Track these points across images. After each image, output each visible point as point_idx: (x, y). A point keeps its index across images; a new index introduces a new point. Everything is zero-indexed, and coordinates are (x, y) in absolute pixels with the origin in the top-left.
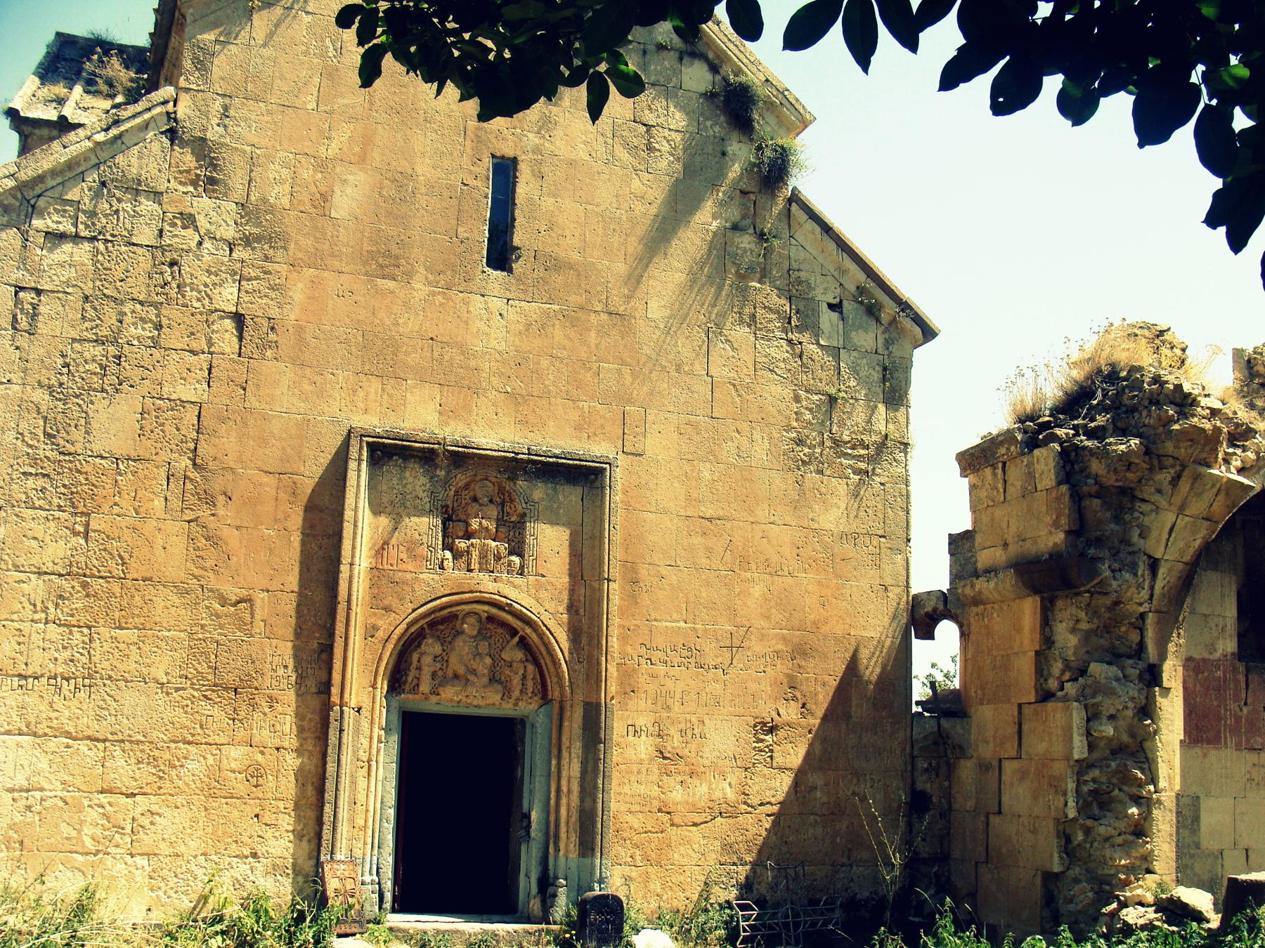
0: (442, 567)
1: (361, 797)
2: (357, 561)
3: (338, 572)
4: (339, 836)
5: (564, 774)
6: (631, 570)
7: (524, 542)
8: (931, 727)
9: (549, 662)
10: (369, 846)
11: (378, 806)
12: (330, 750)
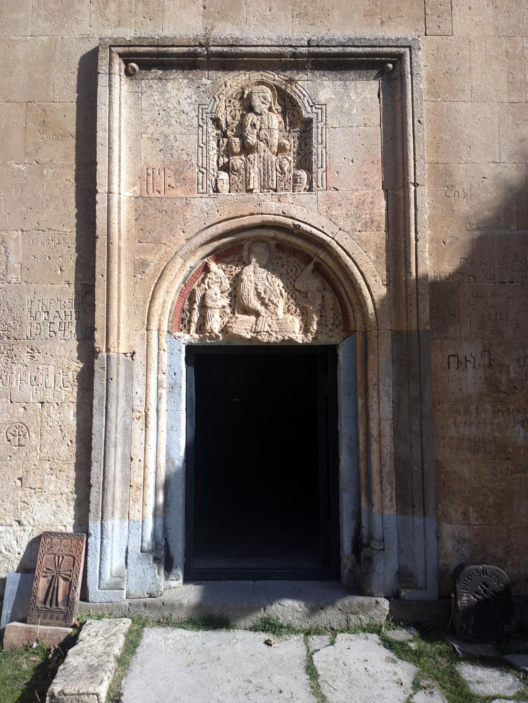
0: (216, 190)
1: (138, 452)
2: (115, 188)
3: (94, 203)
4: (109, 498)
5: (374, 415)
6: (443, 176)
7: (311, 153)
9: (348, 289)
12: (95, 402)
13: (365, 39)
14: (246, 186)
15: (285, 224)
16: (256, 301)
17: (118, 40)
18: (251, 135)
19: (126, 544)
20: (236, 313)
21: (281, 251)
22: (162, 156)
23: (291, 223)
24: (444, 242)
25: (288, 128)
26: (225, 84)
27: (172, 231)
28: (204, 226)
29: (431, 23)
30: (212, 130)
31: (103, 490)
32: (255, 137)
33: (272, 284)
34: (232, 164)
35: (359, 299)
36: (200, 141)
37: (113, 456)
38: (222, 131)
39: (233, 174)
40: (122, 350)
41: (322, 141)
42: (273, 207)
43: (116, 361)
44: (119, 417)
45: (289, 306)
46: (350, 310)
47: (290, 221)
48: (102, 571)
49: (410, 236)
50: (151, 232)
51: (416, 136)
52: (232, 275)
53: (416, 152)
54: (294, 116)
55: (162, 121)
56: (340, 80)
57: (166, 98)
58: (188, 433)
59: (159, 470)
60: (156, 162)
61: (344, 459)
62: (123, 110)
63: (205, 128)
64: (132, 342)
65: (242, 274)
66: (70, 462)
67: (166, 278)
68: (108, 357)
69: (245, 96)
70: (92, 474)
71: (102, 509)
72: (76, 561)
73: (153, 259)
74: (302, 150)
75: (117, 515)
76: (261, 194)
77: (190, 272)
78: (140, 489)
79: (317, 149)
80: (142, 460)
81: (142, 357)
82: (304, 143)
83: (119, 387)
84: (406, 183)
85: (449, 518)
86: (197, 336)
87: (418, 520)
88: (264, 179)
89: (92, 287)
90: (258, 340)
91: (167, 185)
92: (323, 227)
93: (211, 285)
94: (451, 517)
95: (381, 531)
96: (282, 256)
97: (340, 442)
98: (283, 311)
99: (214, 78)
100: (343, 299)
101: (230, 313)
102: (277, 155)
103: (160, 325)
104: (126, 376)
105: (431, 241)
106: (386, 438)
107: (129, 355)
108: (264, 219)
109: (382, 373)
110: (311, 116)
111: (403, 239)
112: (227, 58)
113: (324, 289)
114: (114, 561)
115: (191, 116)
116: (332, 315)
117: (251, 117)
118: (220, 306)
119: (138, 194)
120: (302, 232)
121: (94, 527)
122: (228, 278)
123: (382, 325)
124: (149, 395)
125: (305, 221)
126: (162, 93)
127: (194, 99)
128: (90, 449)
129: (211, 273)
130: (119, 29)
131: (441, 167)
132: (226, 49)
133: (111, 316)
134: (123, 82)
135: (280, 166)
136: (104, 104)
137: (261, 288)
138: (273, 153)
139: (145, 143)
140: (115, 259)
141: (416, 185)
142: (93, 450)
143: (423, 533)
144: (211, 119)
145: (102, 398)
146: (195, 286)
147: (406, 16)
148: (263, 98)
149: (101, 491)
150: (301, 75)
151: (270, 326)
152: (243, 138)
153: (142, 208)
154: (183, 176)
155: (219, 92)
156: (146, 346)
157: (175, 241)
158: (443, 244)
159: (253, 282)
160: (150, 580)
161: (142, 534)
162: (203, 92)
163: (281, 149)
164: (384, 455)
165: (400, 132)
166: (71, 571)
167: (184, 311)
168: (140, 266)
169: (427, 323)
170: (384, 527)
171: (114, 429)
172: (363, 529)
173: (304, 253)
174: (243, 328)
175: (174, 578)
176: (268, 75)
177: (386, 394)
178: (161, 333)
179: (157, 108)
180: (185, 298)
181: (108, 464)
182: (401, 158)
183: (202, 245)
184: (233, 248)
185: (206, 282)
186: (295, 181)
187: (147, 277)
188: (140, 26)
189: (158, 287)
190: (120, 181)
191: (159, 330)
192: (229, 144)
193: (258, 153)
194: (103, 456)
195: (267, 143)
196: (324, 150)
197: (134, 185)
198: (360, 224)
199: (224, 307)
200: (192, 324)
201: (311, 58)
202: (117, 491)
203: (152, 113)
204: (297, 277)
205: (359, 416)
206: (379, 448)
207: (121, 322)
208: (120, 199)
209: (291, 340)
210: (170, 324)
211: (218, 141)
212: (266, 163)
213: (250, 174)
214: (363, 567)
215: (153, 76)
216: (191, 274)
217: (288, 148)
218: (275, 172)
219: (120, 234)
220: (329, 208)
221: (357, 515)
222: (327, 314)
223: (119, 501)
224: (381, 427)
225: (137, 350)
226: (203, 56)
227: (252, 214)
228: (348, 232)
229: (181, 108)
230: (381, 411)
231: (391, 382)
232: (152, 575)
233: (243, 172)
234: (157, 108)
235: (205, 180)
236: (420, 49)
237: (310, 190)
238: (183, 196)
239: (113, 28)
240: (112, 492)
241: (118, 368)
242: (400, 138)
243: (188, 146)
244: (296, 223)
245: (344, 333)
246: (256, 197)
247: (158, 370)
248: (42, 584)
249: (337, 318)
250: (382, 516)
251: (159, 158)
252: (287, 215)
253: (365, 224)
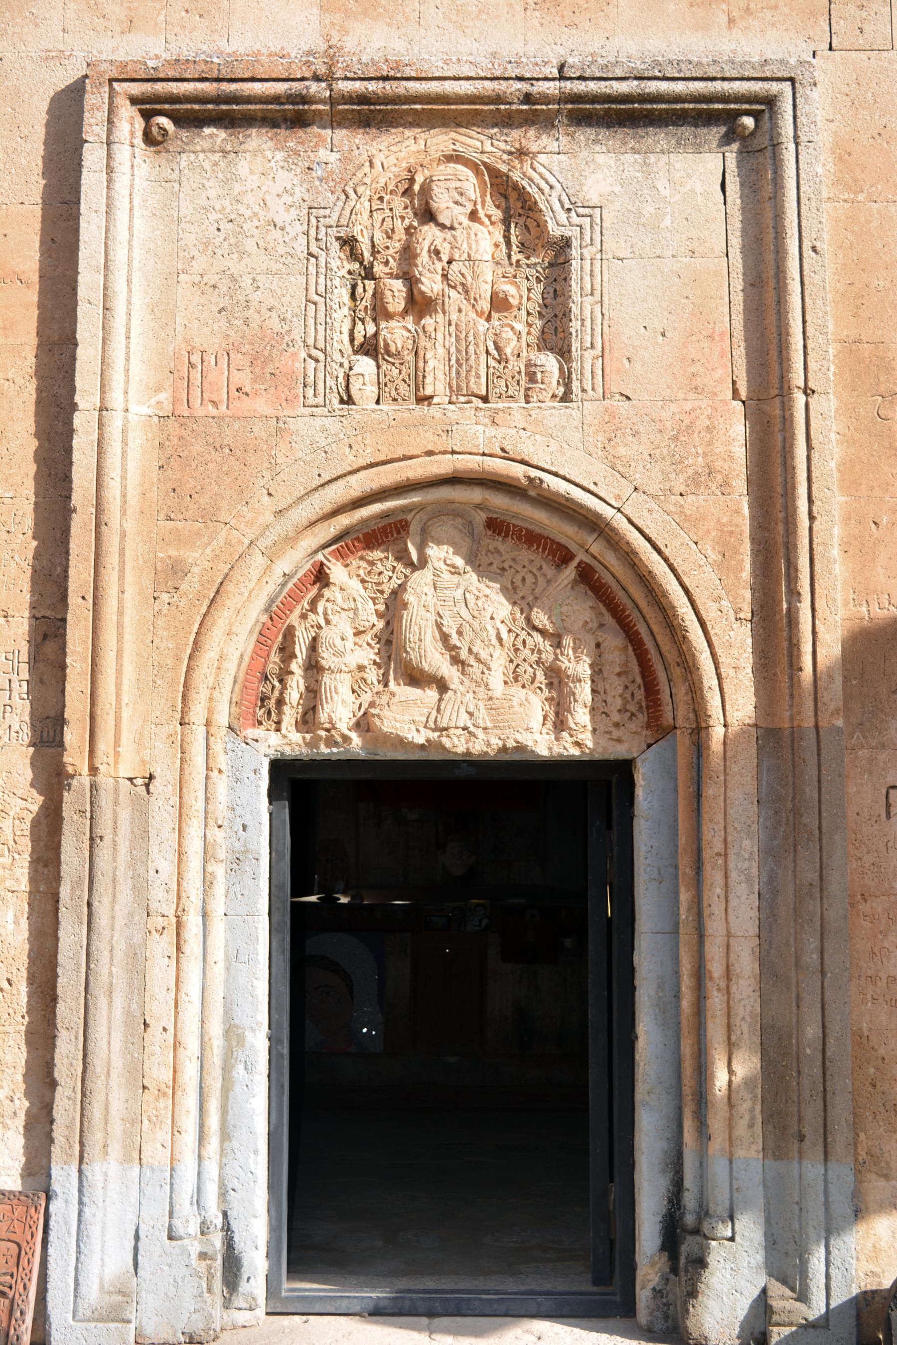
0: (348, 400)
1: (159, 1010)
2: (116, 399)
3: (70, 432)
4: (96, 1113)
5: (715, 927)
7: (566, 314)
9: (656, 628)
10: (189, 1137)
11: (216, 1029)
12: (65, 891)
13: (690, 62)
14: (417, 389)
15: (508, 477)
16: (438, 656)
17: (129, 68)
18: (428, 275)
19: (135, 1220)
20: (392, 684)
21: (499, 534)
22: (223, 323)
23: (520, 475)
24: (875, 523)
25: (514, 259)
26: (371, 162)
28: (318, 482)
29: (842, 22)
30: (339, 263)
31: (84, 1095)
32: (439, 278)
33: (476, 613)
34: (385, 340)
35: (681, 653)
36: (312, 289)
37: (105, 1018)
38: (361, 263)
39: (387, 361)
40: (125, 771)
41: (592, 289)
42: (476, 438)
43: (111, 798)
44: (117, 927)
45: (518, 665)
46: (662, 676)
47: (518, 471)
48: (80, 1278)
49: (795, 509)
50: (195, 496)
51: (806, 282)
52: (382, 592)
53: (808, 318)
54: (529, 231)
55: (225, 244)
56: (634, 151)
57: (236, 193)
58: (274, 970)
59: (208, 1053)
60: (209, 335)
61: (647, 1032)
62: (137, 222)
63: (322, 260)
64: (148, 751)
65: (405, 589)
66: (7, 1028)
67: (228, 603)
68: (94, 787)
69: (416, 187)
70: (57, 1056)
71: (81, 1136)
72: (23, 1253)
73: (199, 559)
74: (546, 306)
75: (115, 1151)
76: (452, 407)
77: (283, 585)
78: (165, 1094)
79: (581, 305)
80: (171, 1028)
81: (170, 787)
82: (552, 290)
84: (786, 387)
85: (883, 1164)
86: (296, 737)
87: (813, 1170)
88: (458, 373)
89: (59, 623)
90: (444, 748)
91: (233, 388)
92: (595, 484)
93: (331, 617)
94: (888, 1163)
95: (727, 1196)
96: (502, 548)
97: (637, 993)
98: (502, 678)
99: (346, 148)
100: (647, 651)
101: (376, 683)
102: (489, 319)
103: (210, 711)
104: (132, 832)
105: (847, 519)
106: (742, 982)
107: (139, 781)
108: (459, 466)
109: (735, 829)
110: (568, 233)
111: (781, 516)
112: (374, 104)
113: (601, 626)
114: (108, 1260)
115: (292, 234)
116: (620, 690)
117: (429, 234)
118: (353, 666)
119: (167, 409)
120: (546, 494)
121: (63, 1177)
122: (373, 599)
123: (736, 714)
124: (186, 876)
125: (554, 469)
126: (226, 182)
127: (298, 196)
128: (54, 999)
129: (332, 587)
130: (130, 36)
131: (866, 350)
132: (372, 86)
133: (101, 692)
134: (138, 161)
135: (495, 343)
136: (96, 211)
137: (451, 623)
138: (480, 314)
140: (112, 559)
141: (808, 391)
142: (60, 1000)
143: (822, 1199)
144: (337, 239)
145: (78, 883)
146: (294, 618)
147: (786, 5)
148: (457, 192)
149: (79, 1096)
150: (545, 140)
151: (471, 714)
152: (411, 281)
153: (175, 441)
154: (270, 368)
155: (355, 180)
156: (178, 761)
157: (249, 516)
158: (873, 526)
159: (432, 609)
160: (190, 1304)
161: (171, 1198)
162: (321, 180)
163: (499, 303)
164: (738, 1022)
165: (772, 272)
166: (12, 1276)
167: (266, 678)
169: (837, 711)
170: (735, 1187)
171: (106, 953)
172: (686, 1194)
173: (552, 541)
174: (407, 718)
175: (244, 1305)
176: (469, 141)
177: (743, 877)
178: (212, 730)
179: (213, 216)
180: (271, 647)
181: (92, 1035)
182: (774, 329)
183: (312, 524)
184: (384, 529)
185: (320, 609)
186: (532, 377)
187: (184, 599)
188: (177, 29)
189: (208, 622)
190: (127, 382)
191: (208, 724)
192: (377, 295)
193: (444, 313)
194: (82, 1016)
195: (467, 292)
196: (597, 308)
197: (158, 390)
198: (682, 478)
199: (361, 668)
200: (286, 709)
201: (566, 103)
202: (113, 1096)
203: (203, 227)
204: (536, 598)
205: (682, 931)
206: (725, 1005)
207: (123, 704)
208: (126, 421)
209: (521, 748)
210: (235, 709)
211: (354, 287)
212: (463, 336)
213: (425, 362)
214: (683, 1279)
215: (206, 144)
216: (286, 590)
217: (514, 302)
218: (483, 357)
219: (125, 502)
220: (610, 440)
221: (675, 1165)
222: (607, 687)
223: (119, 1122)
224: (732, 955)
225: (159, 770)
226: (322, 101)
227: (430, 453)
228: (654, 497)
229: (270, 215)
230: (731, 918)
231: (756, 849)
232: (196, 1292)
233: (410, 358)
234: (213, 216)
235: (321, 375)
236: (815, 85)
237: (566, 398)
238: (270, 412)
239: (116, 36)
240: (104, 1098)
241: (115, 812)
242: (772, 283)
243: (283, 299)
244: (534, 473)
245: (649, 732)
246: (438, 415)
247: (206, 818)
249: (633, 695)
250: (731, 1163)
251: (216, 327)
252: (511, 455)
253: (694, 479)
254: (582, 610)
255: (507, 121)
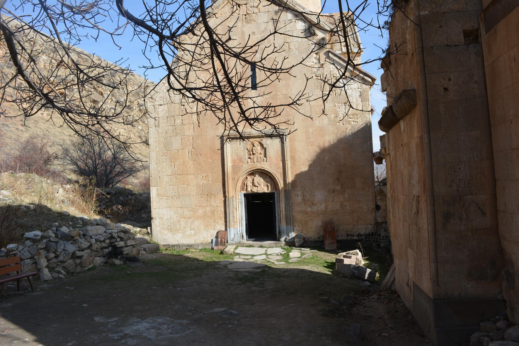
1: (235, 215)
6: (293, 158)
8: (378, 188)
27: (239, 172)
73: (236, 177)
79: (267, 153)
83: (231, 203)
87: (289, 227)
114: (232, 236)
121: (228, 229)
139: (233, 154)
148: (256, 144)
163: (260, 153)
168: (234, 179)
184: (253, 173)
202: (232, 223)
248: (220, 240)
254: (269, 180)
255: (260, 137)
